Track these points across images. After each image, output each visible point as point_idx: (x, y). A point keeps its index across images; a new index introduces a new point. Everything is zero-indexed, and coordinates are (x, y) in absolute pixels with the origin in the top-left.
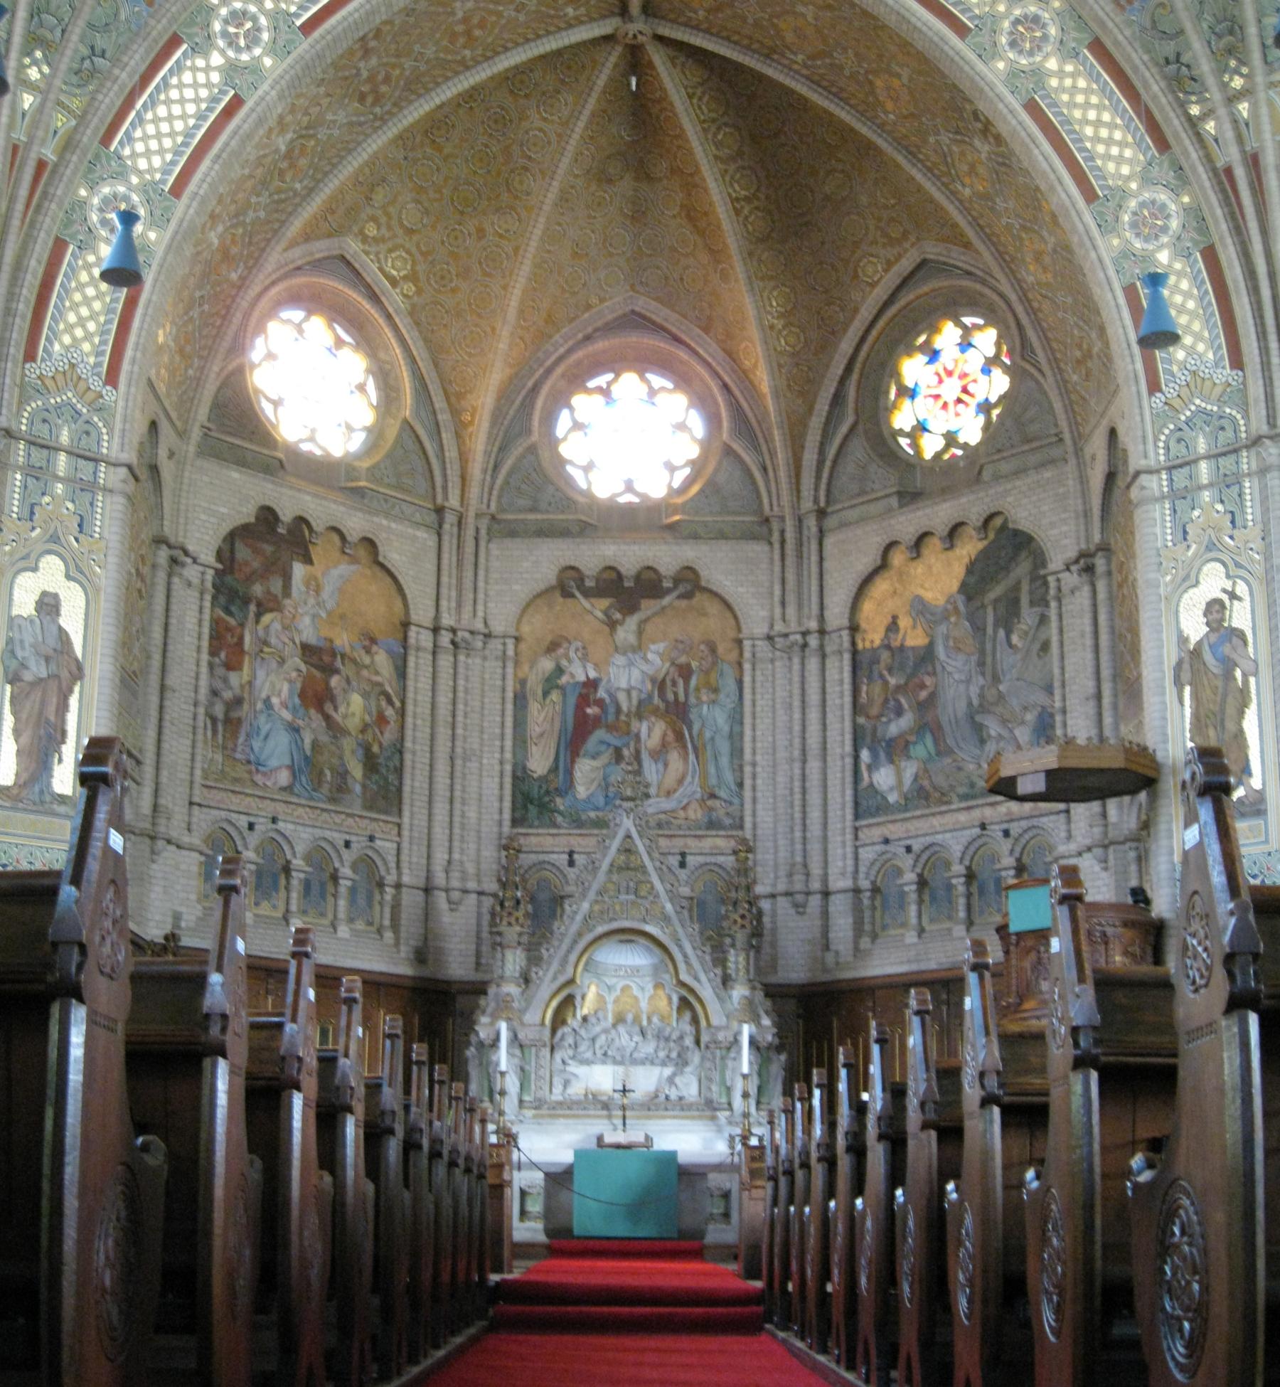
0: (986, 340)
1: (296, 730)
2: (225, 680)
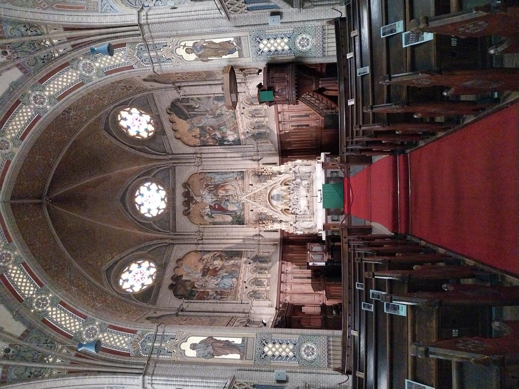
2: (211, 295)
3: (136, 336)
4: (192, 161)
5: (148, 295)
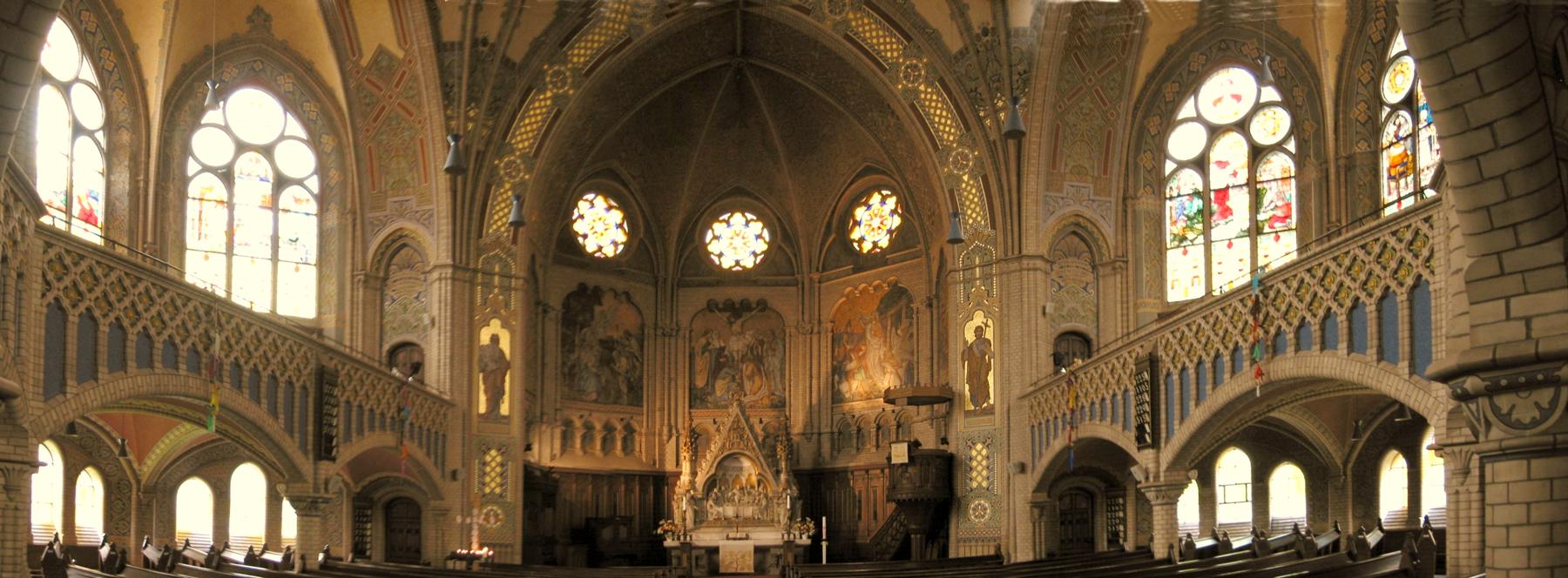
0: (892, 202)
1: (598, 376)
3: (508, 245)
4: (806, 317)
5: (568, 246)
